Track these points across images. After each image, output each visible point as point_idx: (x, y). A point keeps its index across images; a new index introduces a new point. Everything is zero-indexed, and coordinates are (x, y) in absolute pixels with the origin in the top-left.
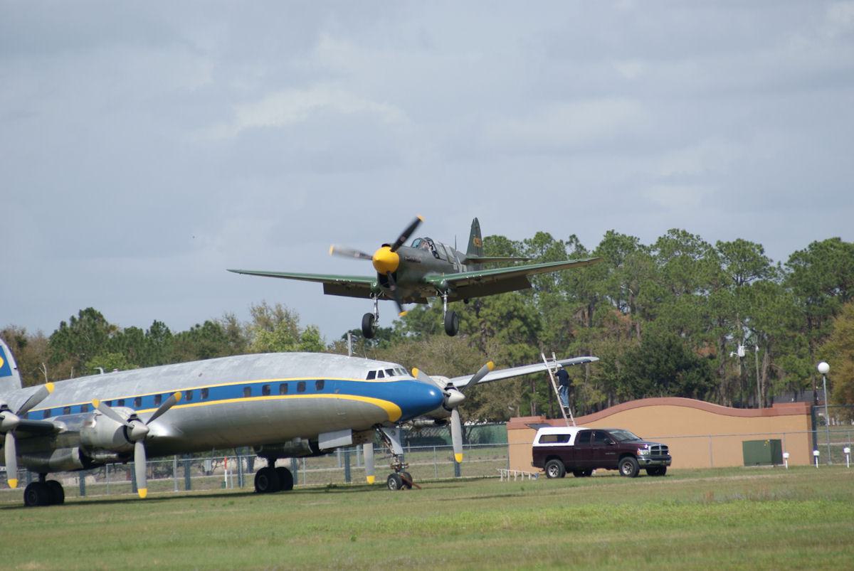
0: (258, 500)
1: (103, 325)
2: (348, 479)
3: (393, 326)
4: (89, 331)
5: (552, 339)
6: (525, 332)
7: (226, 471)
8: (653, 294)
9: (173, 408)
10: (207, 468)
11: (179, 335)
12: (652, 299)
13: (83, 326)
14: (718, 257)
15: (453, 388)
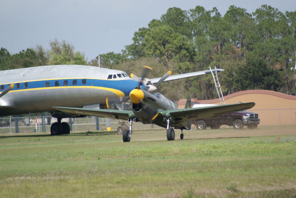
0: (52, 139)
2: (98, 129)
3: (122, 53)
5: (201, 60)
6: (188, 56)
7: (36, 124)
8: (253, 38)
9: (10, 92)
10: (27, 122)
11: (14, 55)
12: (252, 40)
14: (287, 19)
15: (151, 84)
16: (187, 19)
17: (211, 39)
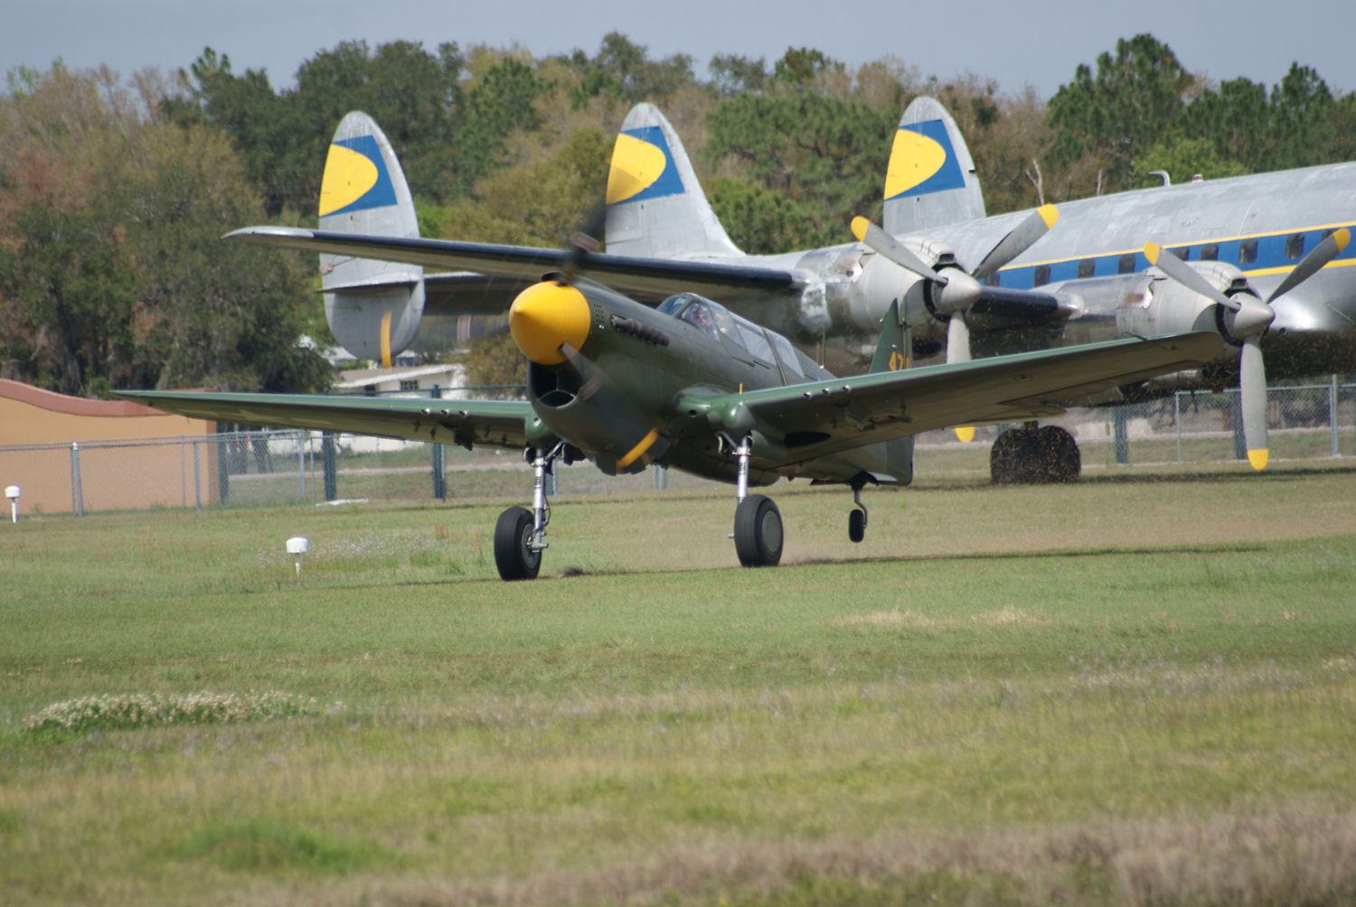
1: (1173, 76)
4: (1141, 87)
9: (1331, 264)
13: (1127, 77)
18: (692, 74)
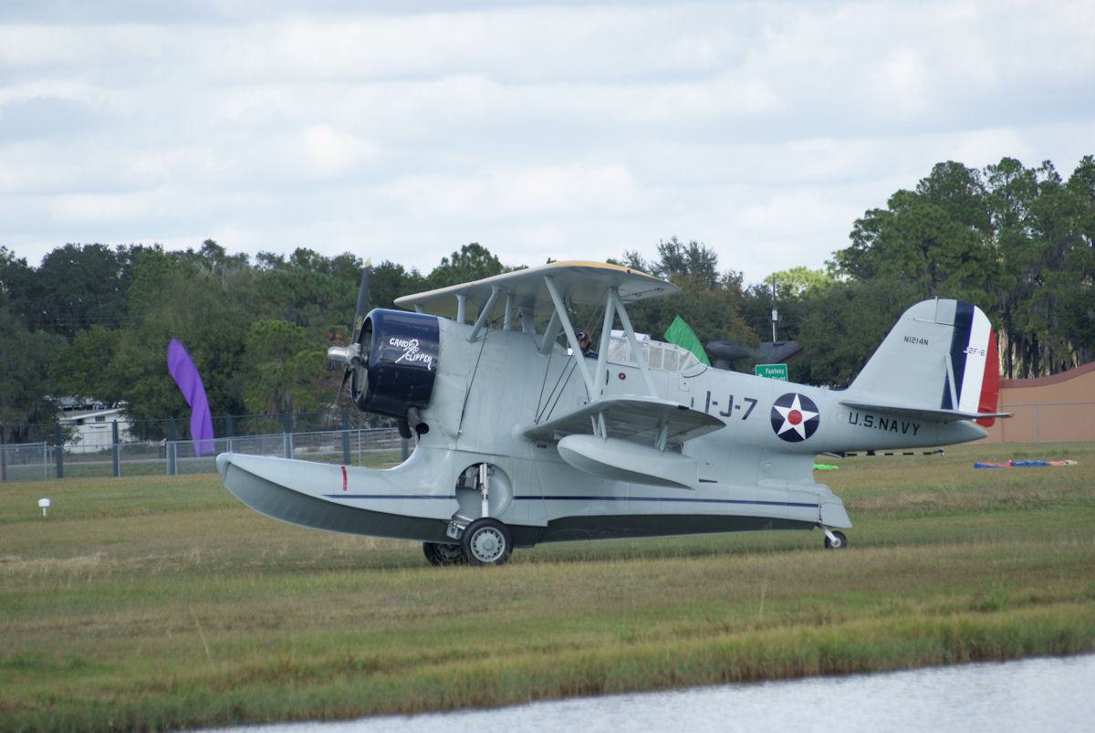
16: (979, 189)
17: (1035, 235)
18: (248, 263)
